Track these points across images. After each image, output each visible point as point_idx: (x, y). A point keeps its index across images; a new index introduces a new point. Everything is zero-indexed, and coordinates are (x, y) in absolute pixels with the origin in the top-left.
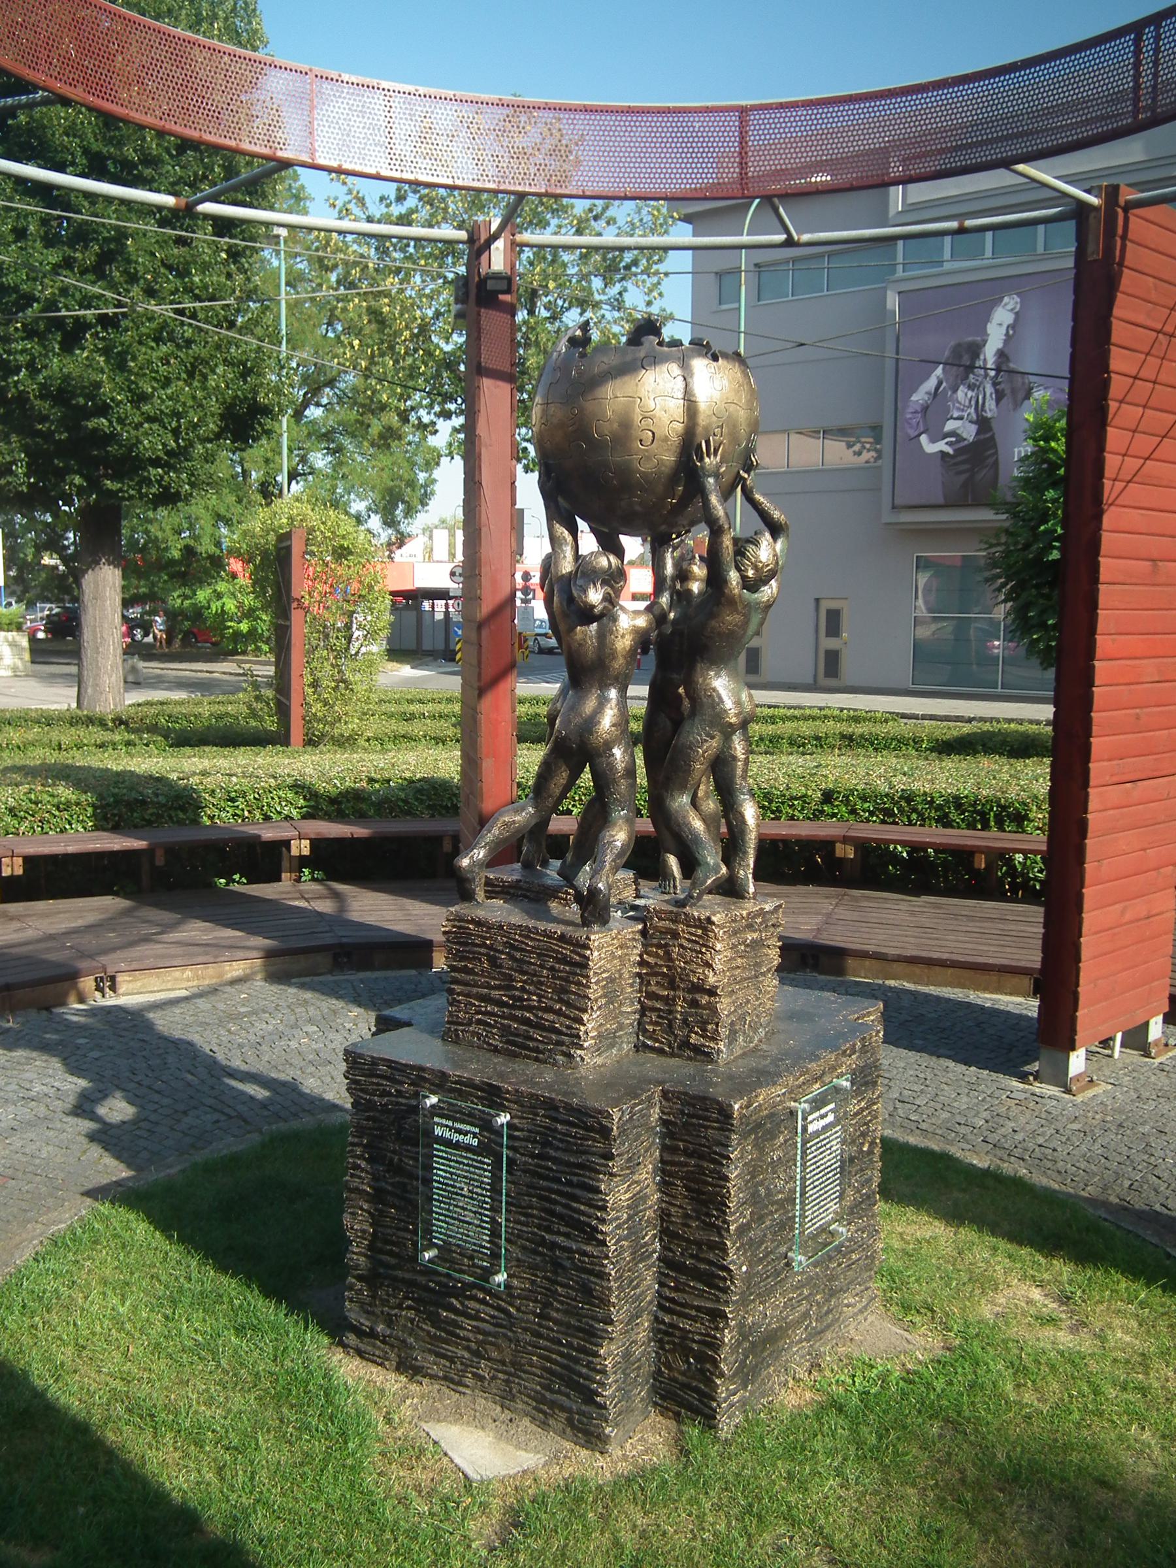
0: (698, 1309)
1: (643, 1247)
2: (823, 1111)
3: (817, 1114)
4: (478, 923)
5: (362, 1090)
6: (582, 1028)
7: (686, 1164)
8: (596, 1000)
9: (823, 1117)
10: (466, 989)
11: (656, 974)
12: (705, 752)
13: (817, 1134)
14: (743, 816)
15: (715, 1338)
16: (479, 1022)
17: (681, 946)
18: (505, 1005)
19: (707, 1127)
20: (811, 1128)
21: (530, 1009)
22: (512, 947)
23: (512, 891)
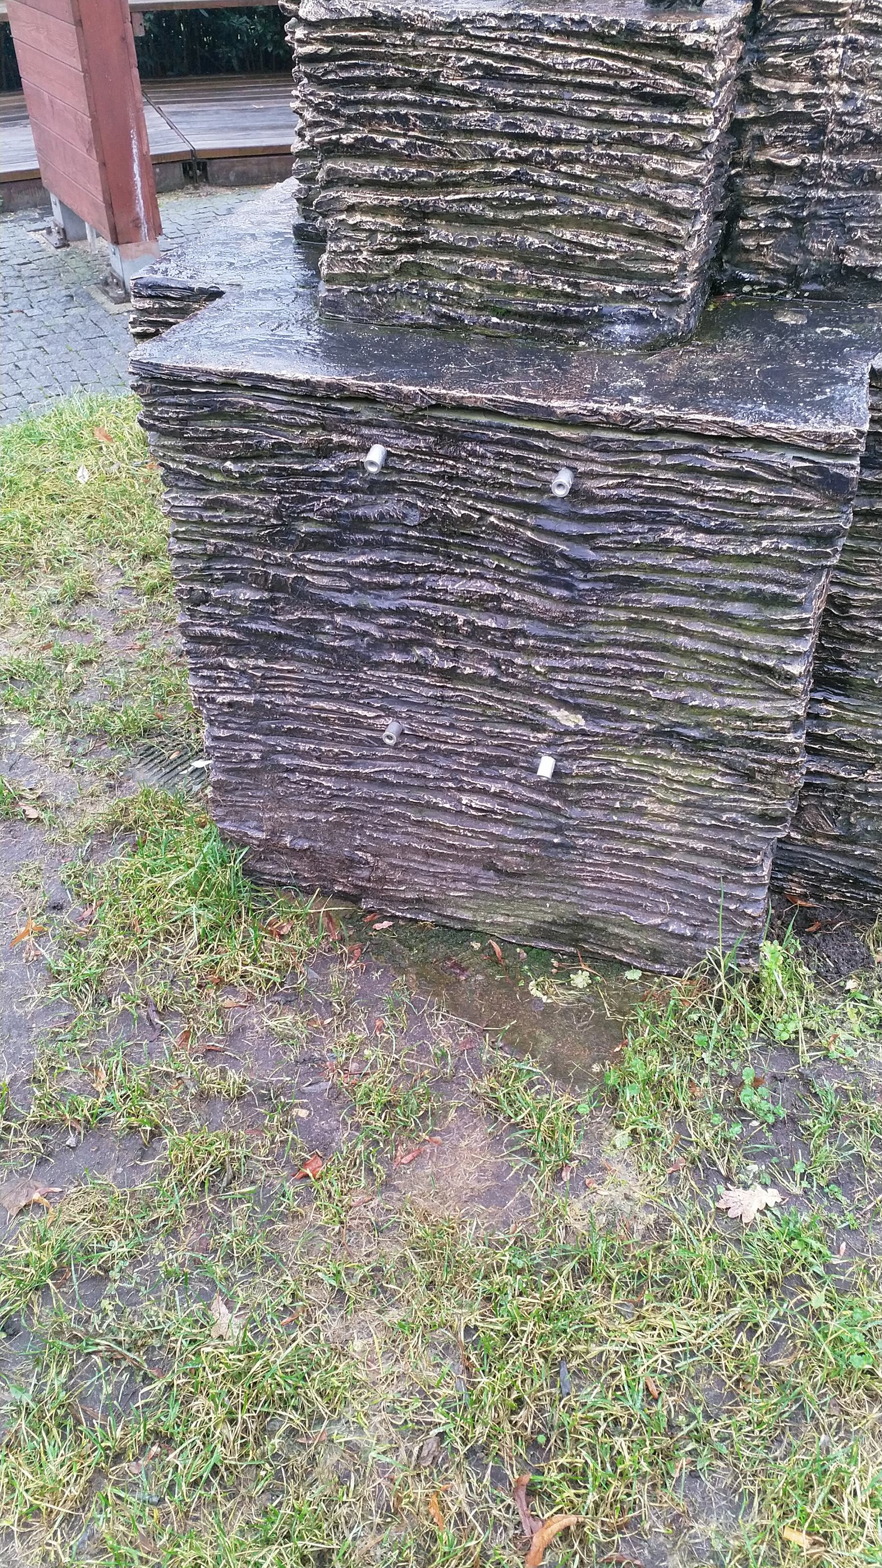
6: (675, 256)
10: (370, 198)
17: (852, 44)
22: (489, 73)
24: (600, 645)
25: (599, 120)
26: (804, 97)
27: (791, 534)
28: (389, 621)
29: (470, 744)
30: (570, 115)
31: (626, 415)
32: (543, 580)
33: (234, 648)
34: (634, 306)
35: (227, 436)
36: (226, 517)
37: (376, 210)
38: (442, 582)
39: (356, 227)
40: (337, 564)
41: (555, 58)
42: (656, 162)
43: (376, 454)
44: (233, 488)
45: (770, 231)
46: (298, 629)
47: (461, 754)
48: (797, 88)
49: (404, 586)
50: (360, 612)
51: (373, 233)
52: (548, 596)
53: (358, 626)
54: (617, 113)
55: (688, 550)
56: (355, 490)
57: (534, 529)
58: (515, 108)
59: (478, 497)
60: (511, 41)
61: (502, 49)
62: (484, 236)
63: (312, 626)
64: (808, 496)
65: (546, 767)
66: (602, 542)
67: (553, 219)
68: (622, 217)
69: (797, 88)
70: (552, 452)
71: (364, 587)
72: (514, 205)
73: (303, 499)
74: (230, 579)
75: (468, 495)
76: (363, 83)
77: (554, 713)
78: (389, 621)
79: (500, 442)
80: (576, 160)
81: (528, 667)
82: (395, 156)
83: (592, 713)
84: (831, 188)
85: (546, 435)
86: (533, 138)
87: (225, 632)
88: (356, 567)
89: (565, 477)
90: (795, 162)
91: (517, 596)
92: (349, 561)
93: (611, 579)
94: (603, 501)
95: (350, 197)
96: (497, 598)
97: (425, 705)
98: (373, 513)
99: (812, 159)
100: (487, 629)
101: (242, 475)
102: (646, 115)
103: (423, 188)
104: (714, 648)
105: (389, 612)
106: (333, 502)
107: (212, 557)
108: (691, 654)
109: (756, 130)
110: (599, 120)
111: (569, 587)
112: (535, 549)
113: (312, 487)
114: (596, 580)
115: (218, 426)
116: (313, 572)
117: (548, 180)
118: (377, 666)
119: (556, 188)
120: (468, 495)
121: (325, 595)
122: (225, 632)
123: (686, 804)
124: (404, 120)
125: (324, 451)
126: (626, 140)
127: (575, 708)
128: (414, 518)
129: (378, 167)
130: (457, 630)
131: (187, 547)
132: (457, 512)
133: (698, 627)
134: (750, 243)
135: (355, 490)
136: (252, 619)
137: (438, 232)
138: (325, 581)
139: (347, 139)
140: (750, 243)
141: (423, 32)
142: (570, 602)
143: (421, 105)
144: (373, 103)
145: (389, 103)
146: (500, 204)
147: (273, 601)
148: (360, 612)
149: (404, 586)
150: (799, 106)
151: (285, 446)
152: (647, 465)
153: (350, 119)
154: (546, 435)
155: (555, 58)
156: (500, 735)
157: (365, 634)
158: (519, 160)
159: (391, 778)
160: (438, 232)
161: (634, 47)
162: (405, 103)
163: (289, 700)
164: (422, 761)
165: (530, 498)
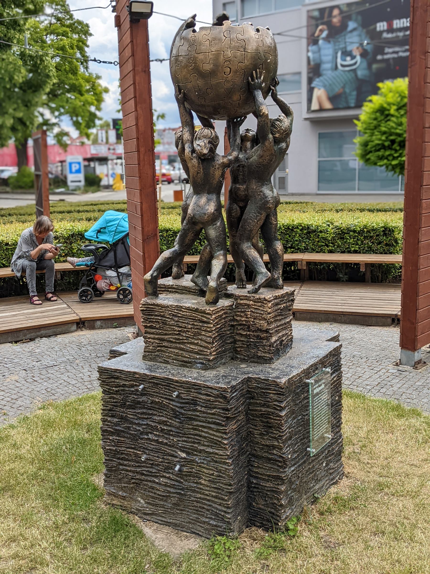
0: (269, 476)
1: (243, 449)
2: (320, 384)
3: (317, 385)
4: (158, 305)
5: (107, 385)
7: (261, 411)
8: (215, 338)
9: (320, 386)
10: (152, 336)
11: (241, 325)
12: (258, 221)
13: (317, 394)
14: (276, 250)
15: (278, 489)
16: (158, 351)
18: (171, 342)
19: (270, 393)
20: (315, 392)
21: (183, 343)
22: (173, 315)
23: (170, 290)
24: (187, 434)
25: (193, 324)
26: (245, 321)
27: (219, 408)
28: (144, 427)
29: (162, 462)
30: (187, 323)
31: (187, 381)
32: (175, 417)
33: (112, 434)
34: (201, 361)
35: (114, 382)
36: (112, 400)
37: (154, 339)
38: (155, 417)
39: (150, 342)
40: (134, 412)
41: (185, 313)
42: (203, 333)
43: (141, 387)
44: (115, 394)
45: (242, 347)
46: (126, 429)
47: (160, 465)
48: (243, 319)
49: (147, 418)
50: (139, 425)
51: (153, 343)
52: (175, 421)
53: (138, 428)
54: (195, 323)
55: (201, 411)
56: (138, 395)
57: (172, 405)
58: (178, 321)
59: (162, 397)
60: (177, 310)
61: (176, 311)
62: (174, 345)
63: (129, 428)
64: (221, 400)
65: (177, 468)
66: (185, 409)
67: (185, 343)
68: (198, 343)
69: (243, 319)
70: (174, 388)
71: (140, 418)
72: (178, 339)
73: (128, 397)
74: (113, 416)
75: (159, 397)
76: (152, 315)
77: (179, 453)
78: (144, 427)
79: (165, 385)
80: (189, 332)
81: (173, 440)
82: (157, 329)
83: (188, 453)
84: (253, 339)
85: (173, 384)
86: (181, 327)
87: (110, 429)
88: (138, 413)
89: (176, 393)
90: (245, 333)
91: (170, 421)
92: (137, 411)
93: (187, 418)
94: (184, 399)
95: (149, 336)
96: (166, 421)
97: (152, 450)
98: (141, 400)
99: (248, 333)
100: (164, 429)
101: (116, 391)
102: (201, 324)
103: (162, 335)
104: (209, 436)
105: (144, 425)
106: (133, 397)
107: (109, 410)
108: (205, 437)
109: (237, 326)
110: (193, 324)
111: (180, 419)
112: (172, 409)
113: (129, 394)
114: (185, 418)
115: (113, 380)
116: (129, 414)
117: (184, 335)
118: (142, 439)
119: (185, 336)
120: (159, 397)
121: (132, 420)
122: (110, 429)
123: (209, 481)
124: (159, 322)
125: (132, 386)
126: (197, 328)
127: (183, 451)
128: (150, 402)
129: (154, 330)
130: (158, 429)
131: (105, 408)
132: (157, 400)
133: (206, 430)
134: (239, 349)
135: (138, 395)
136: (116, 426)
137: (165, 344)
138: (132, 416)
139: (148, 325)
140: (239, 349)
141: (162, 307)
142: (180, 423)
143: (162, 320)
144: (153, 319)
145: (156, 319)
146: (176, 339)
147: (121, 422)
148: (139, 425)
149: (147, 418)
150: (244, 323)
151: (125, 385)
152: (191, 392)
153: (150, 321)
154: (173, 384)
155: (185, 313)
156: (168, 459)
157: (140, 430)
158: (179, 331)
159: (145, 472)
160: (165, 344)
161: (197, 312)
162: (159, 319)
163: (123, 449)
164: (151, 468)
165: (168, 397)
